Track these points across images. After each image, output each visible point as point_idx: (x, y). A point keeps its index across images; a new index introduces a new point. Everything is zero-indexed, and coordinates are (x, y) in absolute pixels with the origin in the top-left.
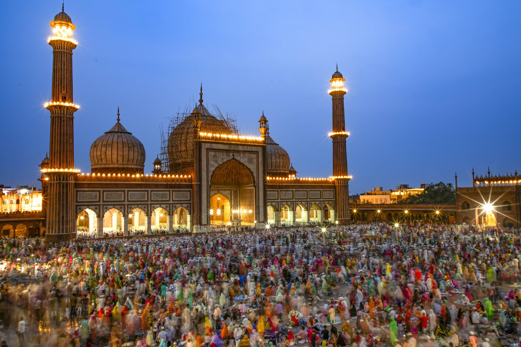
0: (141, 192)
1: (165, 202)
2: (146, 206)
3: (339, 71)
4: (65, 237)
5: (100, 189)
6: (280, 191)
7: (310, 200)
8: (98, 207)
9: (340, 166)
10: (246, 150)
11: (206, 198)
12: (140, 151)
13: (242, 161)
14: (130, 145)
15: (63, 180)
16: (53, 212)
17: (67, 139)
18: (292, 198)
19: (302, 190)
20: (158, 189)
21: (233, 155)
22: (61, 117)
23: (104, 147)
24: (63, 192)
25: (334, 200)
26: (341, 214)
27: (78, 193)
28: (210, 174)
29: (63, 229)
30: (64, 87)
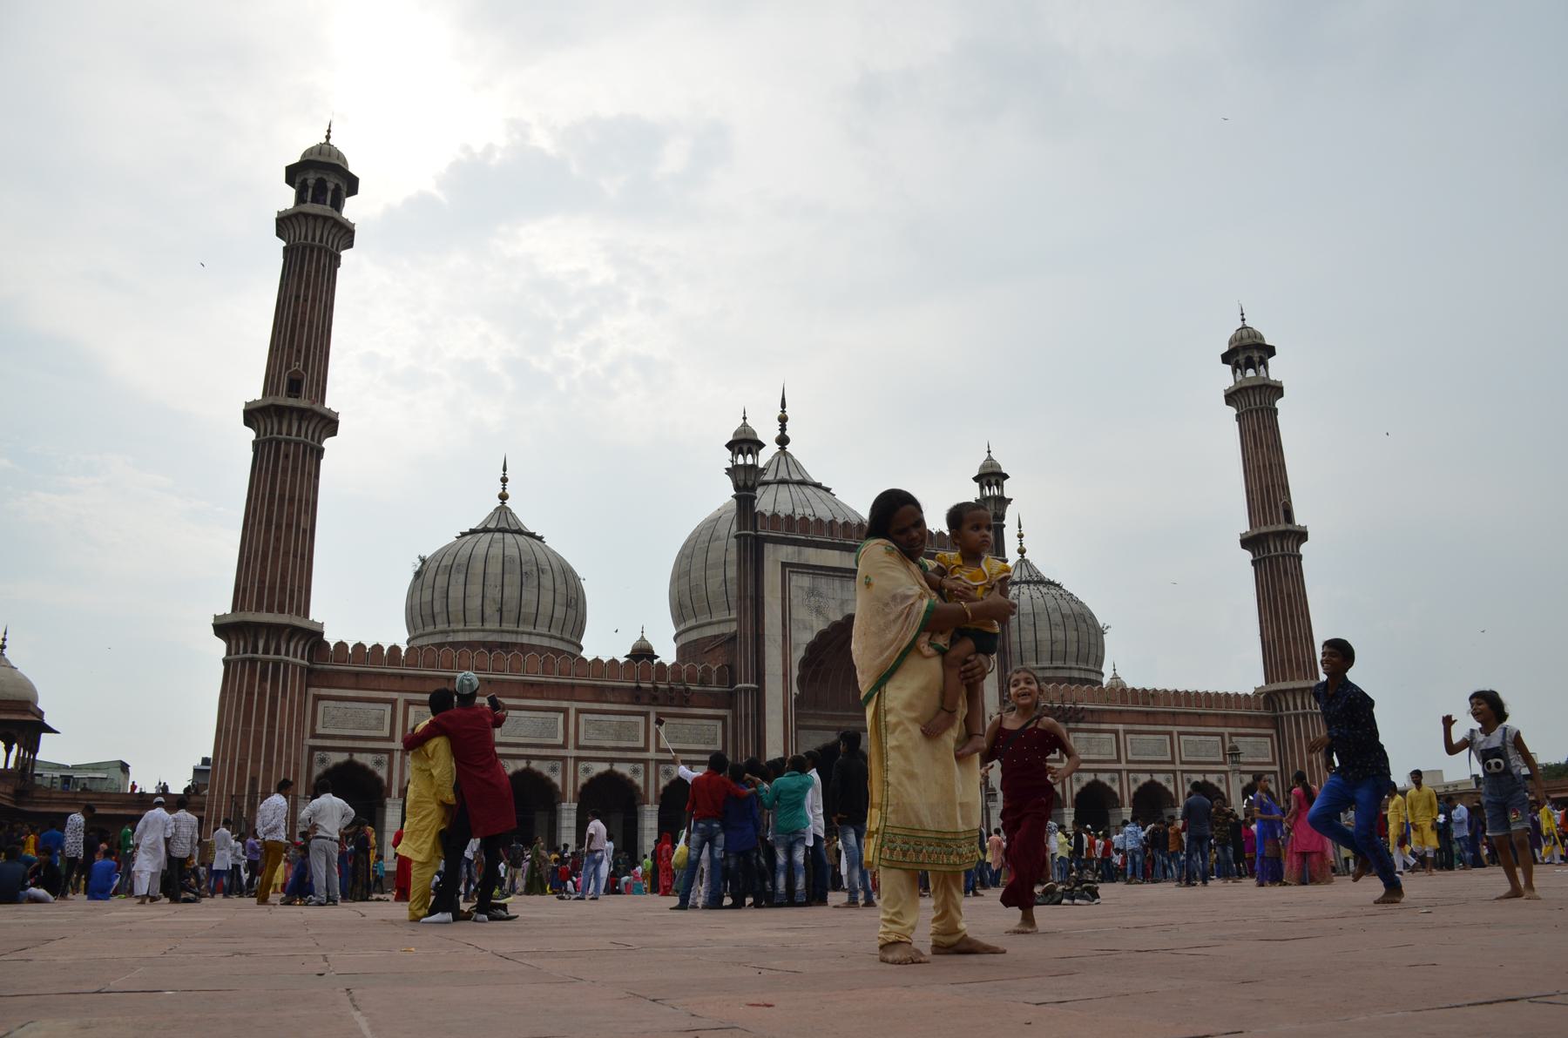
0: (542, 714)
2: (559, 764)
3: (1247, 323)
5: (394, 695)
7: (1186, 767)
8: (386, 757)
9: (1288, 643)
15: (266, 651)
16: (224, 761)
17: (290, 515)
18: (1115, 757)
19: (1152, 728)
20: (605, 706)
22: (279, 443)
23: (444, 573)
24: (262, 694)
25: (1277, 768)
27: (322, 705)
28: (798, 655)
30: (299, 351)
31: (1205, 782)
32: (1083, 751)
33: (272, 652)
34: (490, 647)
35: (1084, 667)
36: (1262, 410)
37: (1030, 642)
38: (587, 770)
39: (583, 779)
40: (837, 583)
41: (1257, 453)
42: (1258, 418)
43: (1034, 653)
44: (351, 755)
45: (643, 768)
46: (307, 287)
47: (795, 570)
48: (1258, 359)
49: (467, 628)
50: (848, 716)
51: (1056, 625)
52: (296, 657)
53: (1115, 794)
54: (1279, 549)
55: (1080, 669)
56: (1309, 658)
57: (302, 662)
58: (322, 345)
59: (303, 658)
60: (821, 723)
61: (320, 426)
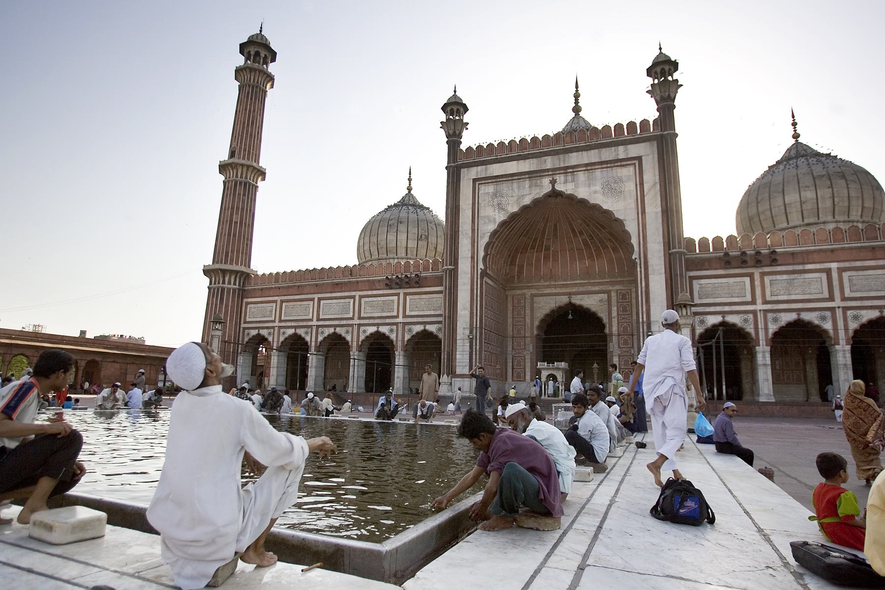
0: (342, 301)
1: (388, 321)
6: (763, 275)
8: (272, 330)
10: (593, 162)
11: (468, 306)
12: (413, 231)
13: (582, 193)
14: (390, 222)
15: (215, 284)
18: (826, 295)
20: (375, 292)
21: (553, 182)
27: (249, 306)
28: (483, 241)
30: (235, 137)
32: (782, 292)
35: (842, 219)
37: (779, 207)
38: (364, 331)
39: (362, 337)
40: (515, 185)
46: (240, 105)
47: (483, 182)
50: (576, 284)
51: (806, 187)
52: (232, 285)
53: (826, 332)
55: (837, 222)
57: (235, 287)
58: (247, 131)
59: (235, 284)
60: (554, 291)
61: (245, 169)
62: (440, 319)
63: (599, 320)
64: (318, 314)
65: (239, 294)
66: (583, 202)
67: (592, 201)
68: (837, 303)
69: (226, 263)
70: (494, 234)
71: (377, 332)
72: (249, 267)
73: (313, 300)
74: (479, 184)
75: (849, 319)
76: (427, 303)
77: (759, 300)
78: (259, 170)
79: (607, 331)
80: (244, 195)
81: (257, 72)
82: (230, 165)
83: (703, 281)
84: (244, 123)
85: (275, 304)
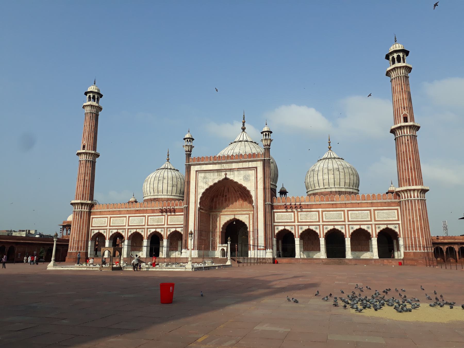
2: (143, 230)
4: (73, 254)
6: (298, 212)
8: (106, 230)
9: (403, 171)
12: (170, 182)
13: (235, 180)
15: (77, 209)
21: (226, 174)
22: (81, 161)
24: (76, 218)
26: (409, 243)
27: (94, 219)
28: (200, 196)
29: (73, 248)
30: (85, 138)
31: (360, 229)
32: (304, 218)
33: (78, 209)
34: (151, 200)
35: (337, 187)
36: (396, 78)
38: (150, 231)
39: (149, 234)
40: (212, 174)
41: (394, 96)
42: (395, 81)
43: (318, 184)
44: (99, 231)
45: (164, 230)
46: (87, 123)
47: (200, 172)
48: (396, 56)
49: (148, 195)
54: (401, 134)
56: (412, 177)
58: (91, 136)
59: (87, 209)
60: (229, 213)
62: (182, 226)
63: (246, 225)
64: (128, 224)
65: (89, 214)
66: (236, 183)
67: (239, 183)
68: (321, 223)
69: (83, 199)
70: (204, 194)
71: (156, 232)
72: (93, 200)
73: (126, 217)
74: (198, 173)
75: (324, 229)
76: (177, 219)
77: (296, 221)
78: (97, 155)
79: (248, 230)
80: (90, 167)
81: (95, 107)
82: (84, 153)
83: (278, 213)
84: (89, 132)
85: (107, 218)
